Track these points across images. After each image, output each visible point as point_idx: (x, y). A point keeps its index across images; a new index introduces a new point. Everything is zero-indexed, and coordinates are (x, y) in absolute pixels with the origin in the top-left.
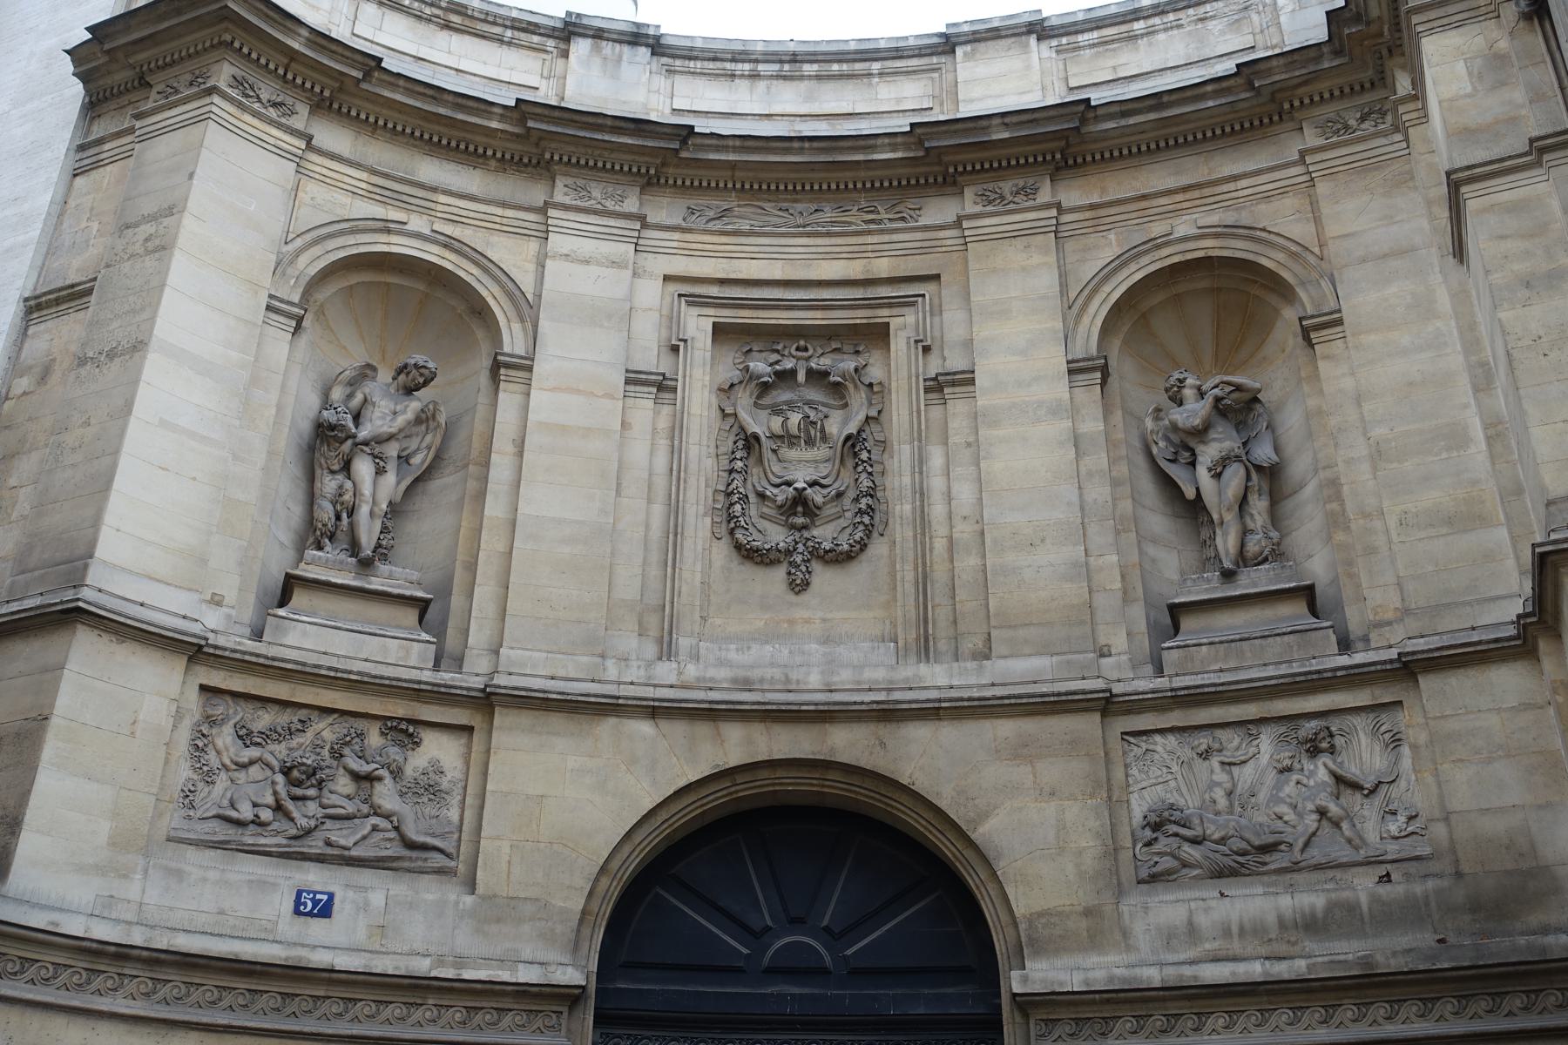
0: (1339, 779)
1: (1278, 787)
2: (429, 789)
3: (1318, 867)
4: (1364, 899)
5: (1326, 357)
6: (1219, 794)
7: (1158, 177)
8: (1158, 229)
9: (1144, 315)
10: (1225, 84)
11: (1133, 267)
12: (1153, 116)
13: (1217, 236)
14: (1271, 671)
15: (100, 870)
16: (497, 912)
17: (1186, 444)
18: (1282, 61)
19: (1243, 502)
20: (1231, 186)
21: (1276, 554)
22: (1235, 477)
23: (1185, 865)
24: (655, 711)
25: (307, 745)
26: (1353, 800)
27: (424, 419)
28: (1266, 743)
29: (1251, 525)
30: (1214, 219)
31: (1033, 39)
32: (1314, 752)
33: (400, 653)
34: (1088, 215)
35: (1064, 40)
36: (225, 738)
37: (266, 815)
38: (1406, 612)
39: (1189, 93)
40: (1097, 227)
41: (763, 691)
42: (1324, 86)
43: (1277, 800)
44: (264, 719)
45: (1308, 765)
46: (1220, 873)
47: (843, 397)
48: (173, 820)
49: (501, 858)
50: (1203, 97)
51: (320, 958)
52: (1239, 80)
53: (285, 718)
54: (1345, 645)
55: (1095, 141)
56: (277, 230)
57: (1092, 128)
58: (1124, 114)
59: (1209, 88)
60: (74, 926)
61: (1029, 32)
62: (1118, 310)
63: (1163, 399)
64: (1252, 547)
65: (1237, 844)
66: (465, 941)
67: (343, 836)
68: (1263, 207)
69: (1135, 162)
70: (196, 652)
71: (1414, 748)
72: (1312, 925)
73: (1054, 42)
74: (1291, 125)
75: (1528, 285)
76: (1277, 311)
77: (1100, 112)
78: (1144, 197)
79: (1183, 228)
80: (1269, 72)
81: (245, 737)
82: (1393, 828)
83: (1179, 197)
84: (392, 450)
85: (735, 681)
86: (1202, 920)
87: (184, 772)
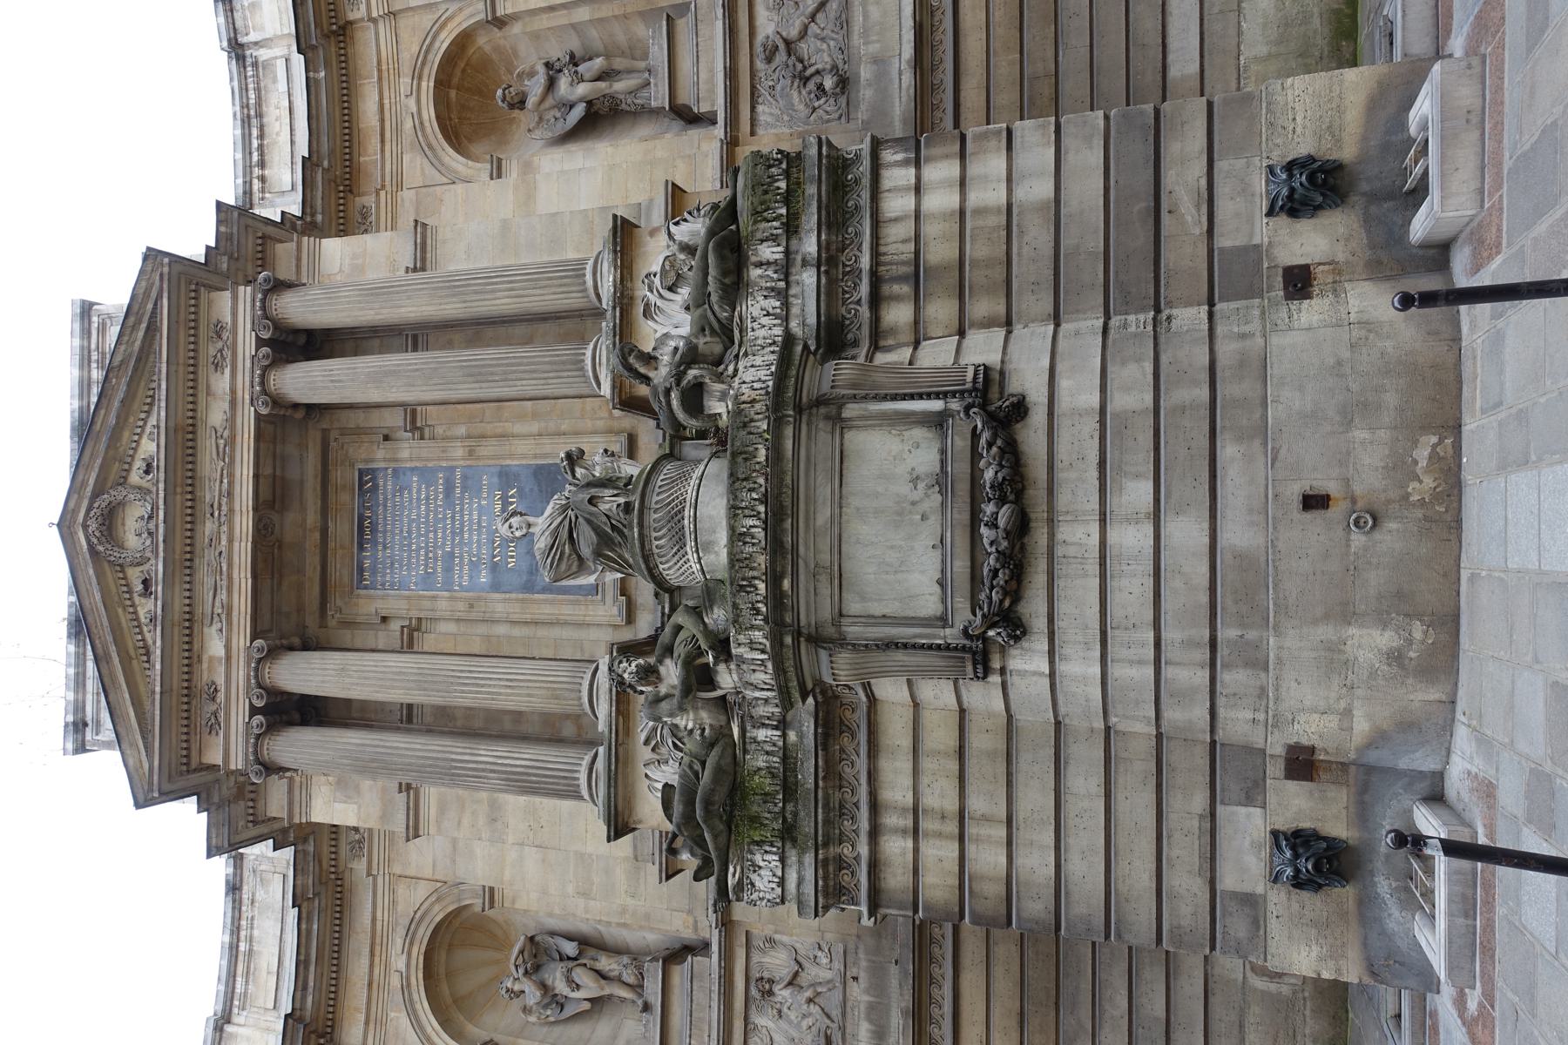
0: (790, 984)
1: (790, 1022)
3: (844, 1014)
4: (866, 998)
5: (513, 902)
7: (358, 968)
8: (395, 981)
9: (455, 1001)
10: (304, 915)
11: (418, 1006)
12: (312, 968)
13: (411, 944)
14: (715, 1005)
17: (553, 1000)
18: (299, 877)
19: (602, 975)
20: (379, 924)
21: (636, 957)
22: (581, 975)
26: (804, 979)
28: (762, 1020)
29: (616, 973)
30: (399, 942)
31: (229, 1028)
32: (770, 993)
34: (372, 1026)
35: (236, 1003)
38: (690, 912)
39: (303, 940)
40: (382, 1023)
42: (326, 850)
43: (798, 1026)
45: (779, 999)
50: (309, 932)
52: (305, 904)
54: (703, 948)
55: (318, 1009)
57: (308, 1014)
58: (305, 988)
59: (304, 926)
61: (221, 1030)
62: (446, 1023)
63: (517, 1004)
64: (631, 980)
68: (400, 908)
69: (342, 982)
73: (235, 1010)
74: (347, 875)
75: (494, 820)
77: (298, 1006)
78: (370, 984)
79: (401, 964)
80: (305, 886)
82: (825, 961)
83: (377, 960)
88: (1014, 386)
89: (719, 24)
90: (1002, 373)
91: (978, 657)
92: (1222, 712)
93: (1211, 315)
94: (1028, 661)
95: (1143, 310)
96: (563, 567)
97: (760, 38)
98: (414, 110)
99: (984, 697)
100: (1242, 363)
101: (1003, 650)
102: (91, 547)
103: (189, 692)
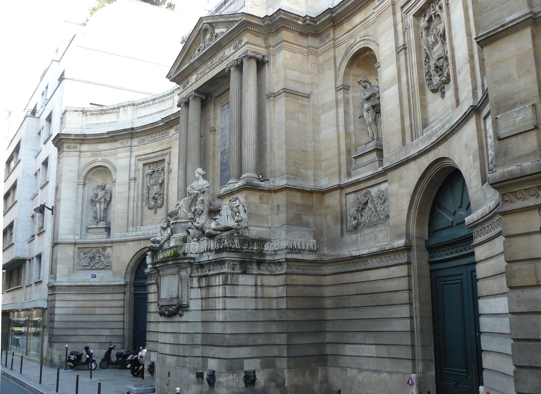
2: (108, 257)
15: (68, 276)
16: (115, 274)
24: (133, 241)
25: (90, 255)
27: (106, 192)
33: (102, 237)
36: (82, 254)
37: (88, 264)
44: (86, 250)
48: (77, 267)
49: (115, 266)
51: (94, 284)
53: (89, 249)
56: (77, 171)
60: (64, 284)
66: (111, 279)
67: (97, 266)
70: (75, 244)
81: (84, 254)
84: (103, 200)
87: (77, 260)
88: (185, 313)
89: (370, 173)
90: (188, 310)
93: (198, 357)
95: (202, 341)
97: (370, 189)
98: (357, 41)
100: (185, 362)
102: (200, 29)
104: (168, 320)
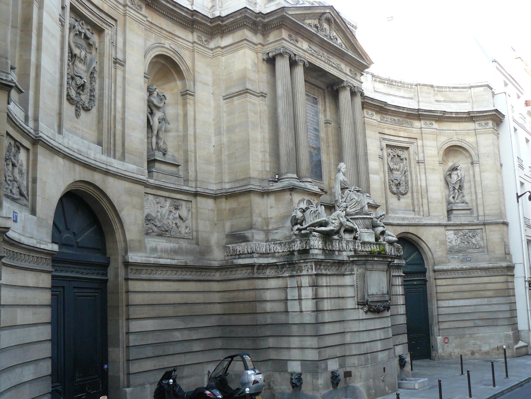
1: (169, 215)
4: (184, 247)
6: (159, 214)
23: (153, 231)
39: (181, 8)
41: (84, 156)
46: (160, 235)
47: (91, 50)
59: (185, 10)
65: (163, 229)
71: (192, 213)
72: (175, 252)
76: (175, 80)
80: (198, 16)
82: (187, 231)
83: (168, 34)
85: (78, 150)
86: (159, 248)
91: (363, 304)
92: (356, 357)
94: (361, 314)
96: (342, 184)
99: (351, 304)
101: (362, 309)
103: (297, 33)
104: (377, 316)
